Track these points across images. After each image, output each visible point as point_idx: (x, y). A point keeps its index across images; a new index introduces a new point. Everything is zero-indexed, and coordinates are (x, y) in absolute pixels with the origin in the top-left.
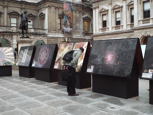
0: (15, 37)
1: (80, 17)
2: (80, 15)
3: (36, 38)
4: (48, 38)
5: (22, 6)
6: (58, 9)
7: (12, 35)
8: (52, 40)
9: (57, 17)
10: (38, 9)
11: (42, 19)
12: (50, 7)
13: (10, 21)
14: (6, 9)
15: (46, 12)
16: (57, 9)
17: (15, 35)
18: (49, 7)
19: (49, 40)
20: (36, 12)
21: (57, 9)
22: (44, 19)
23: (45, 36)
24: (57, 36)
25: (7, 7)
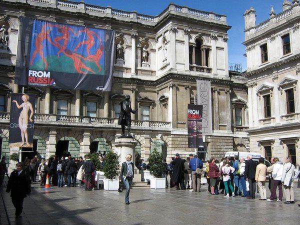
11: (163, 105)
15: (169, 94)
21: (188, 89)
22: (166, 105)
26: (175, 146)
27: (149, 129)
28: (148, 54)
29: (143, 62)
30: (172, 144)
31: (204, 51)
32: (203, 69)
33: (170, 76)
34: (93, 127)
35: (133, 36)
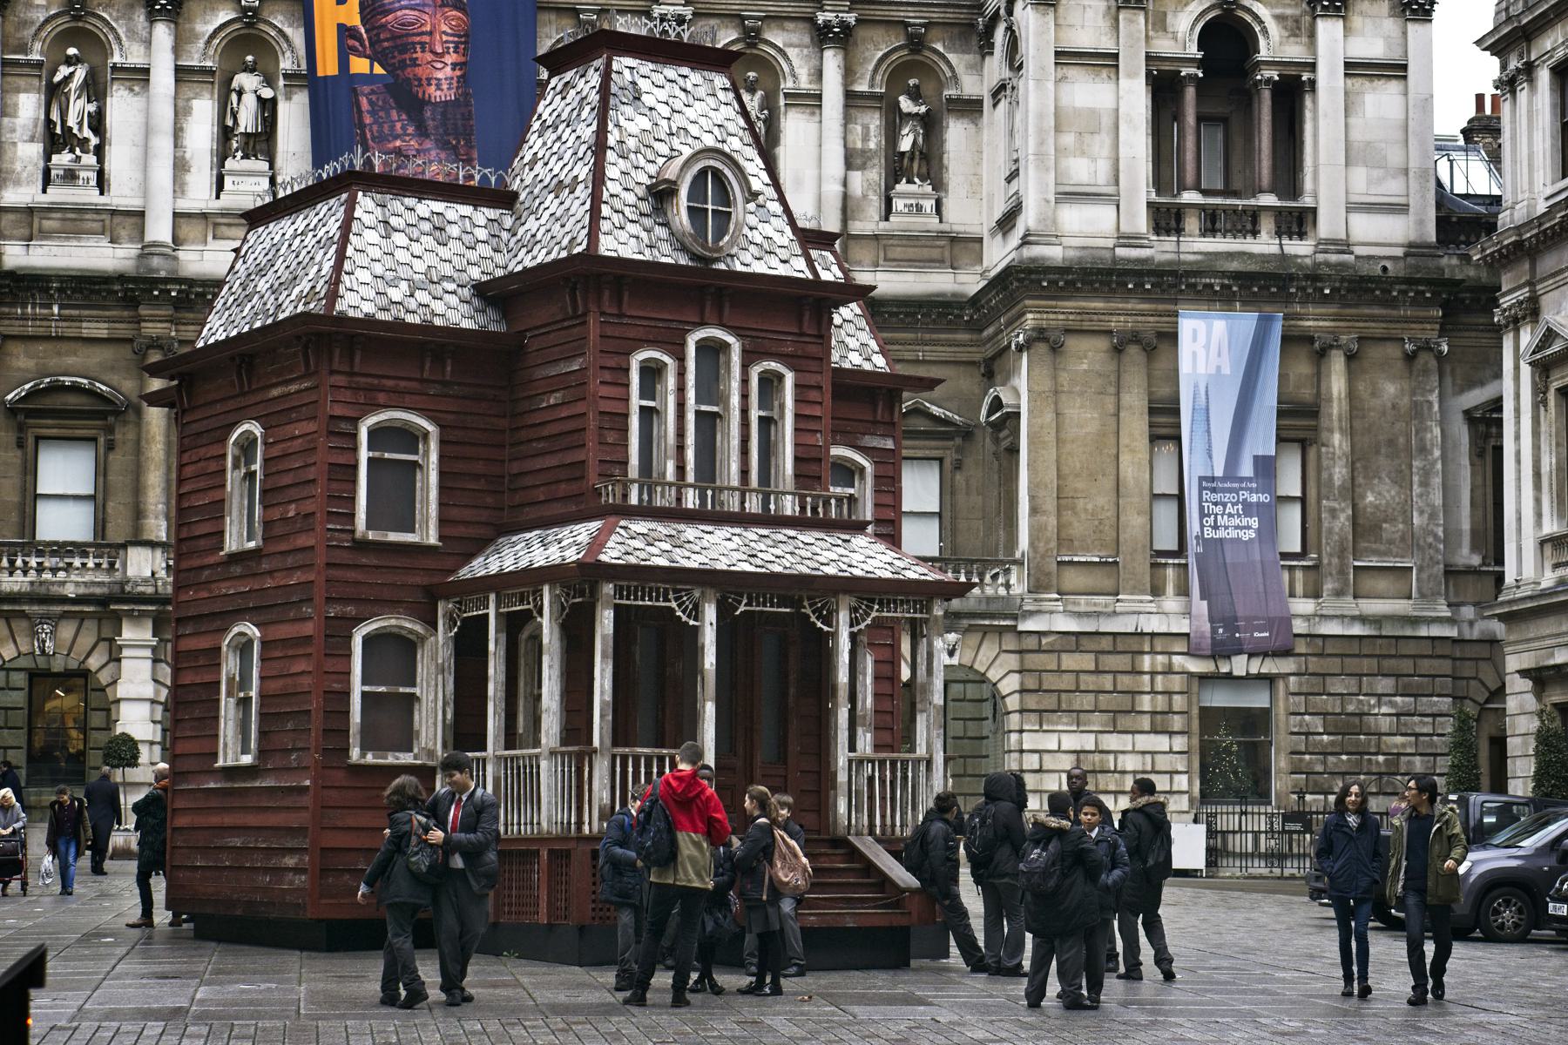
1: (1418, 412)
2: (1413, 393)
4: (1031, 643)
6: (1150, 351)
8: (1069, 662)
12: (1056, 349)
16: (1133, 351)
18: (1046, 340)
19: (1034, 661)
21: (1133, 351)
23: (1001, 631)
26: (1049, 702)
28: (931, 125)
29: (902, 186)
30: (1022, 691)
31: (1266, 95)
32: (1254, 215)
35: (823, 36)
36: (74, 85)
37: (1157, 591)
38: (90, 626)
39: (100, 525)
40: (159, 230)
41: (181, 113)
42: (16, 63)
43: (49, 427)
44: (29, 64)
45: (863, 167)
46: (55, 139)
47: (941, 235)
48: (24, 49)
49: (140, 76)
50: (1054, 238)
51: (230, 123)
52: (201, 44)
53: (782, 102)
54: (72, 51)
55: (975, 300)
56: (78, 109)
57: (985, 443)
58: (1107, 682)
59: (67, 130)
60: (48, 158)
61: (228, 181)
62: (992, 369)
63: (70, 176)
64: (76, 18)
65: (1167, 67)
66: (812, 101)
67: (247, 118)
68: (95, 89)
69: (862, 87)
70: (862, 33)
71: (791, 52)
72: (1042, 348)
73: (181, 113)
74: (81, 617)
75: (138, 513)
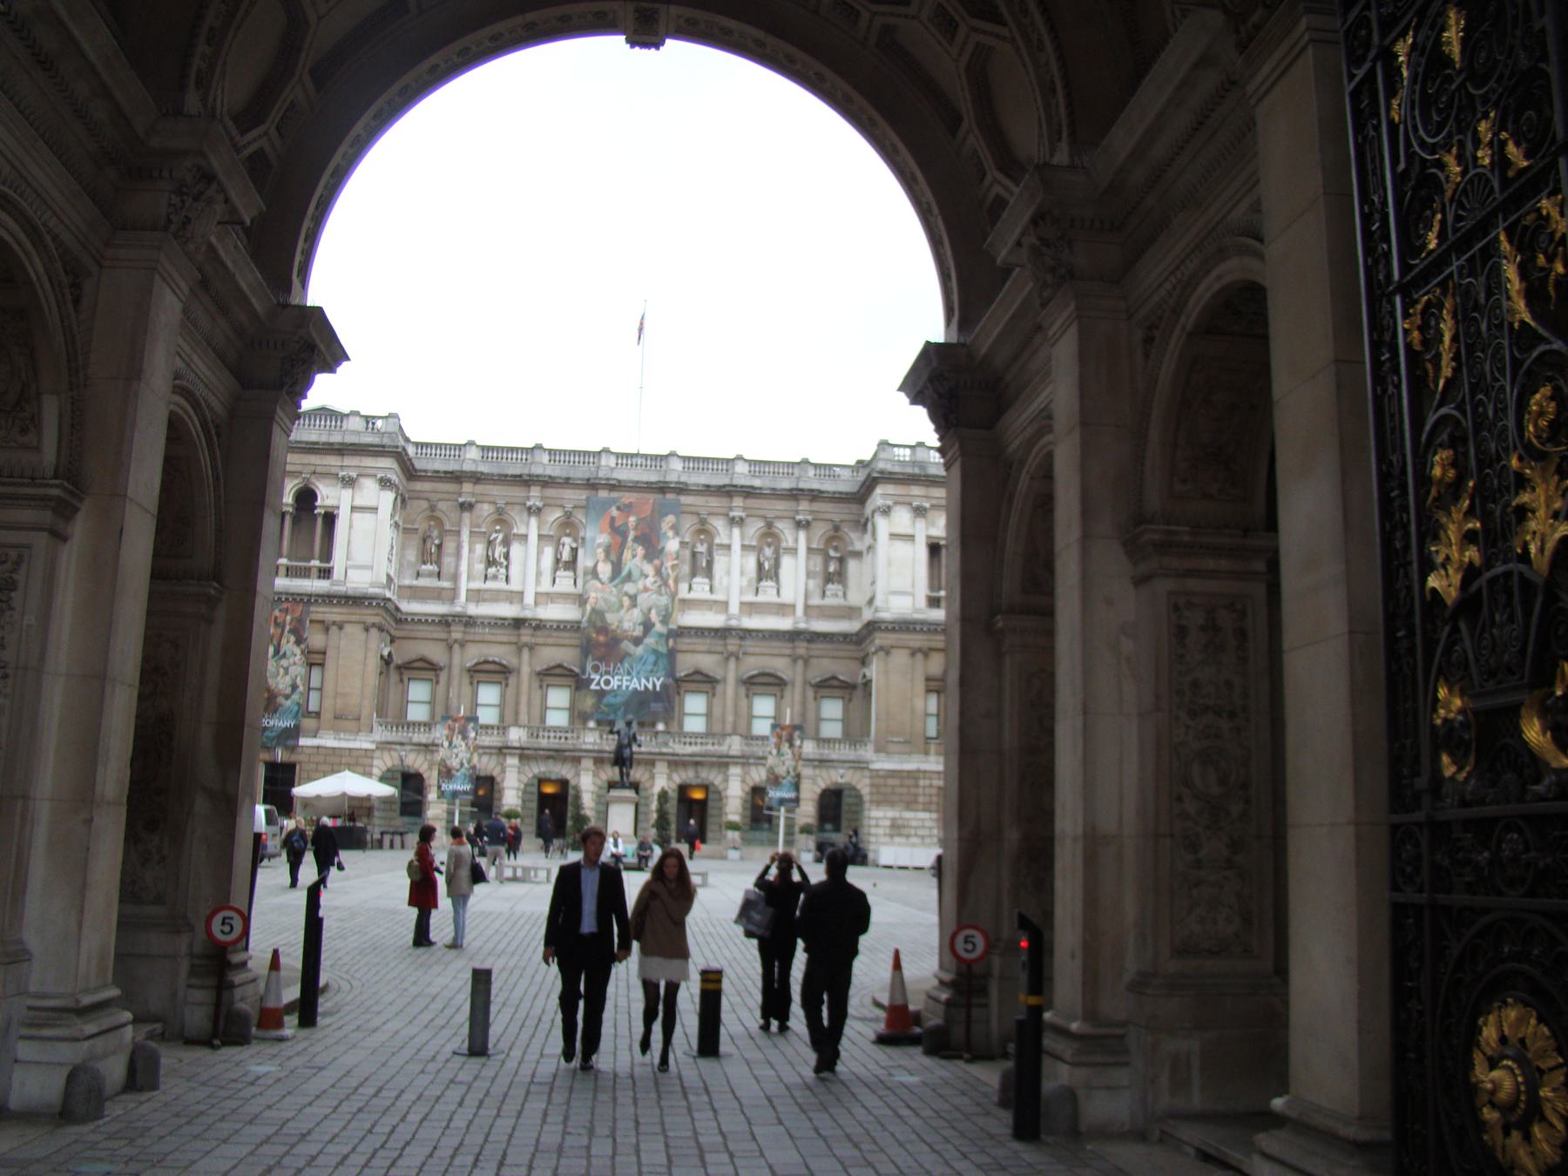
0: (735, 771)
3: (824, 773)
4: (874, 773)
5: (794, 648)
7: (726, 765)
8: (891, 782)
9: (920, 686)
10: (862, 654)
12: (888, 653)
13: (750, 707)
14: (732, 664)
17: (736, 764)
20: (854, 665)
21: (919, 656)
23: (863, 768)
24: (911, 764)
25: (737, 658)
27: (811, 757)
28: (841, 561)
29: (830, 586)
30: (871, 793)
33: (872, 627)
34: (673, 755)
35: (799, 525)
36: (498, 541)
37: (927, 753)
38: (494, 758)
39: (502, 717)
40: (529, 599)
41: (540, 553)
42: (475, 532)
43: (482, 677)
44: (481, 532)
45: (814, 578)
46: (490, 562)
47: (845, 607)
48: (479, 526)
49: (525, 537)
50: (888, 610)
51: (559, 556)
52: (548, 525)
53: (781, 551)
54: (498, 528)
55: (857, 634)
56: (499, 551)
57: (859, 692)
58: (905, 790)
59: (494, 559)
60: (486, 570)
61: (557, 580)
62: (864, 661)
63: (495, 577)
64: (500, 514)
65: (935, 541)
66: (793, 551)
67: (566, 555)
68: (506, 542)
69: (814, 546)
70: (814, 524)
71: (786, 532)
72: (881, 654)
73: (540, 553)
74: (491, 754)
75: (517, 713)
